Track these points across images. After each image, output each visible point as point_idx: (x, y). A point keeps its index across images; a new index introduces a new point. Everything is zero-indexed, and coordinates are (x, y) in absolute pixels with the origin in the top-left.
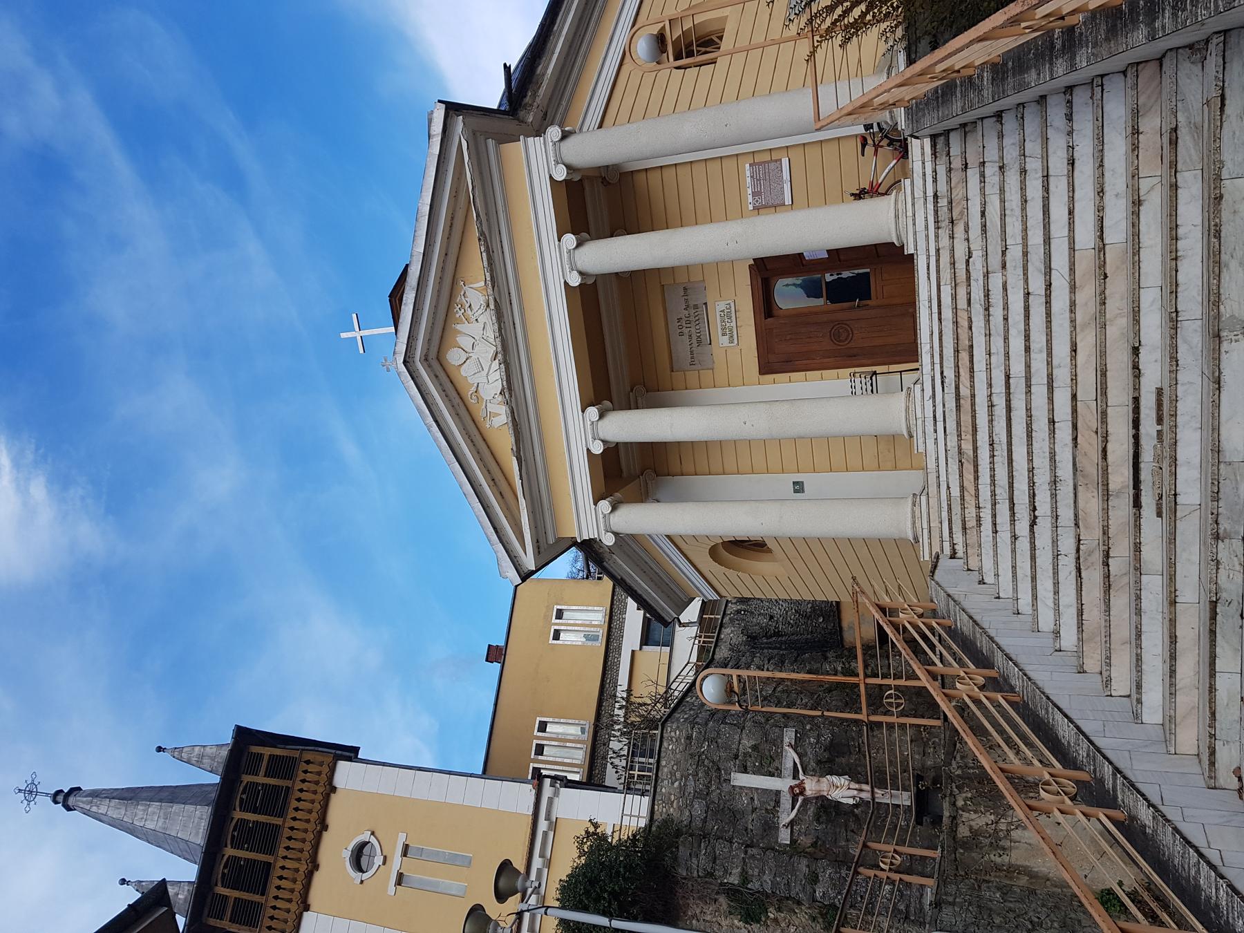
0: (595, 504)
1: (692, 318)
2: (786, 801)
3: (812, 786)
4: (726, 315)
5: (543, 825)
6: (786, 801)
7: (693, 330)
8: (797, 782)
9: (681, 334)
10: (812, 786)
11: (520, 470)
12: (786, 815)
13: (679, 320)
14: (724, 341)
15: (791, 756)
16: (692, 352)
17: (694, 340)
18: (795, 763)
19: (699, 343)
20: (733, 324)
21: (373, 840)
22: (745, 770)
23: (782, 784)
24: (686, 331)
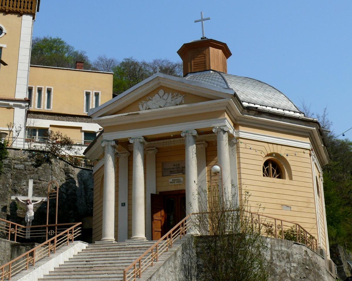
0: (114, 140)
1: (179, 169)
2: (25, 198)
3: (31, 206)
4: (179, 181)
5: (11, 103)
6: (25, 198)
7: (175, 169)
8: (31, 202)
9: (174, 165)
10: (31, 206)
11: (124, 116)
12: (21, 198)
13: (179, 165)
14: (171, 180)
15: (39, 200)
16: (168, 169)
17: (173, 170)
18: (37, 201)
19: (171, 172)
20: (176, 183)
21: (3, 34)
22: (34, 183)
23: (30, 197)
24: (175, 167)
